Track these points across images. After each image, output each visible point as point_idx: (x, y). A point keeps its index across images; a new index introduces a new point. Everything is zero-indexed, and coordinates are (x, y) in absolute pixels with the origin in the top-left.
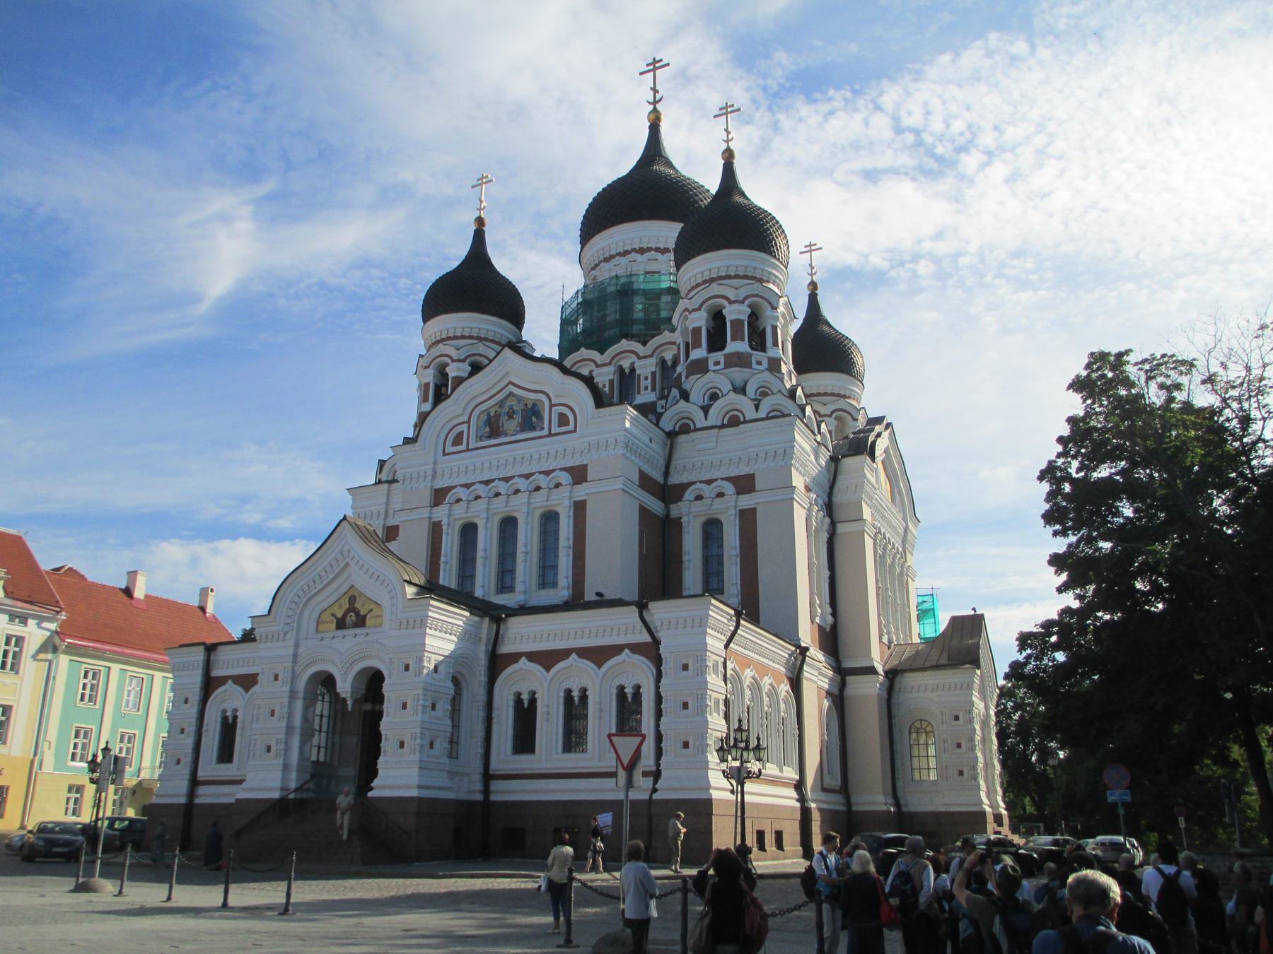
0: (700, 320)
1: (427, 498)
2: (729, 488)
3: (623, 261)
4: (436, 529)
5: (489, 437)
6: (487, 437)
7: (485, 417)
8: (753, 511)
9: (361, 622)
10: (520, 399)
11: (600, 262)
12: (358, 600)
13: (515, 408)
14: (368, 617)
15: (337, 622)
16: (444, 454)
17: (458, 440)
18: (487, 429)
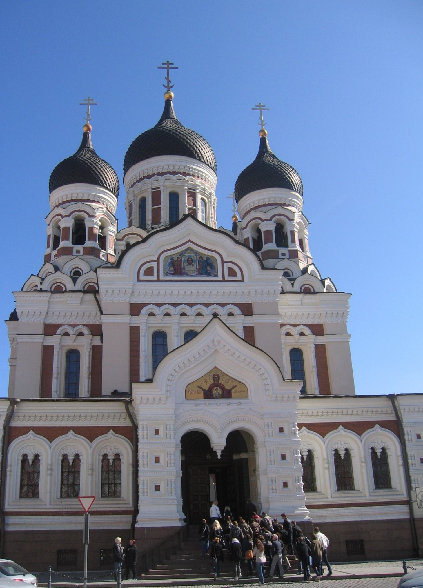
0: (271, 226)
1: (127, 309)
2: (307, 331)
3: (174, 178)
4: (134, 332)
5: (174, 274)
6: (172, 274)
7: (170, 261)
8: (323, 346)
9: (227, 394)
10: (196, 253)
11: (153, 175)
12: (221, 378)
13: (193, 259)
14: (233, 391)
15: (204, 393)
16: (139, 280)
17: (149, 272)
18: (172, 269)
